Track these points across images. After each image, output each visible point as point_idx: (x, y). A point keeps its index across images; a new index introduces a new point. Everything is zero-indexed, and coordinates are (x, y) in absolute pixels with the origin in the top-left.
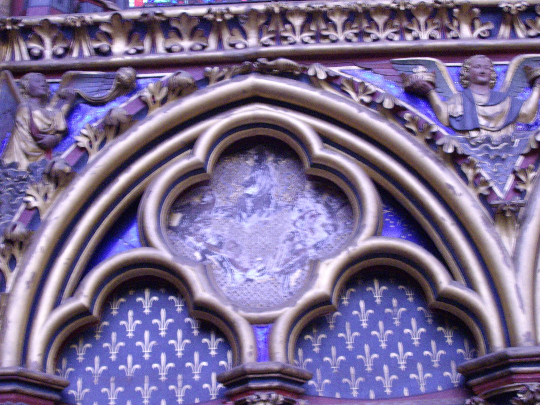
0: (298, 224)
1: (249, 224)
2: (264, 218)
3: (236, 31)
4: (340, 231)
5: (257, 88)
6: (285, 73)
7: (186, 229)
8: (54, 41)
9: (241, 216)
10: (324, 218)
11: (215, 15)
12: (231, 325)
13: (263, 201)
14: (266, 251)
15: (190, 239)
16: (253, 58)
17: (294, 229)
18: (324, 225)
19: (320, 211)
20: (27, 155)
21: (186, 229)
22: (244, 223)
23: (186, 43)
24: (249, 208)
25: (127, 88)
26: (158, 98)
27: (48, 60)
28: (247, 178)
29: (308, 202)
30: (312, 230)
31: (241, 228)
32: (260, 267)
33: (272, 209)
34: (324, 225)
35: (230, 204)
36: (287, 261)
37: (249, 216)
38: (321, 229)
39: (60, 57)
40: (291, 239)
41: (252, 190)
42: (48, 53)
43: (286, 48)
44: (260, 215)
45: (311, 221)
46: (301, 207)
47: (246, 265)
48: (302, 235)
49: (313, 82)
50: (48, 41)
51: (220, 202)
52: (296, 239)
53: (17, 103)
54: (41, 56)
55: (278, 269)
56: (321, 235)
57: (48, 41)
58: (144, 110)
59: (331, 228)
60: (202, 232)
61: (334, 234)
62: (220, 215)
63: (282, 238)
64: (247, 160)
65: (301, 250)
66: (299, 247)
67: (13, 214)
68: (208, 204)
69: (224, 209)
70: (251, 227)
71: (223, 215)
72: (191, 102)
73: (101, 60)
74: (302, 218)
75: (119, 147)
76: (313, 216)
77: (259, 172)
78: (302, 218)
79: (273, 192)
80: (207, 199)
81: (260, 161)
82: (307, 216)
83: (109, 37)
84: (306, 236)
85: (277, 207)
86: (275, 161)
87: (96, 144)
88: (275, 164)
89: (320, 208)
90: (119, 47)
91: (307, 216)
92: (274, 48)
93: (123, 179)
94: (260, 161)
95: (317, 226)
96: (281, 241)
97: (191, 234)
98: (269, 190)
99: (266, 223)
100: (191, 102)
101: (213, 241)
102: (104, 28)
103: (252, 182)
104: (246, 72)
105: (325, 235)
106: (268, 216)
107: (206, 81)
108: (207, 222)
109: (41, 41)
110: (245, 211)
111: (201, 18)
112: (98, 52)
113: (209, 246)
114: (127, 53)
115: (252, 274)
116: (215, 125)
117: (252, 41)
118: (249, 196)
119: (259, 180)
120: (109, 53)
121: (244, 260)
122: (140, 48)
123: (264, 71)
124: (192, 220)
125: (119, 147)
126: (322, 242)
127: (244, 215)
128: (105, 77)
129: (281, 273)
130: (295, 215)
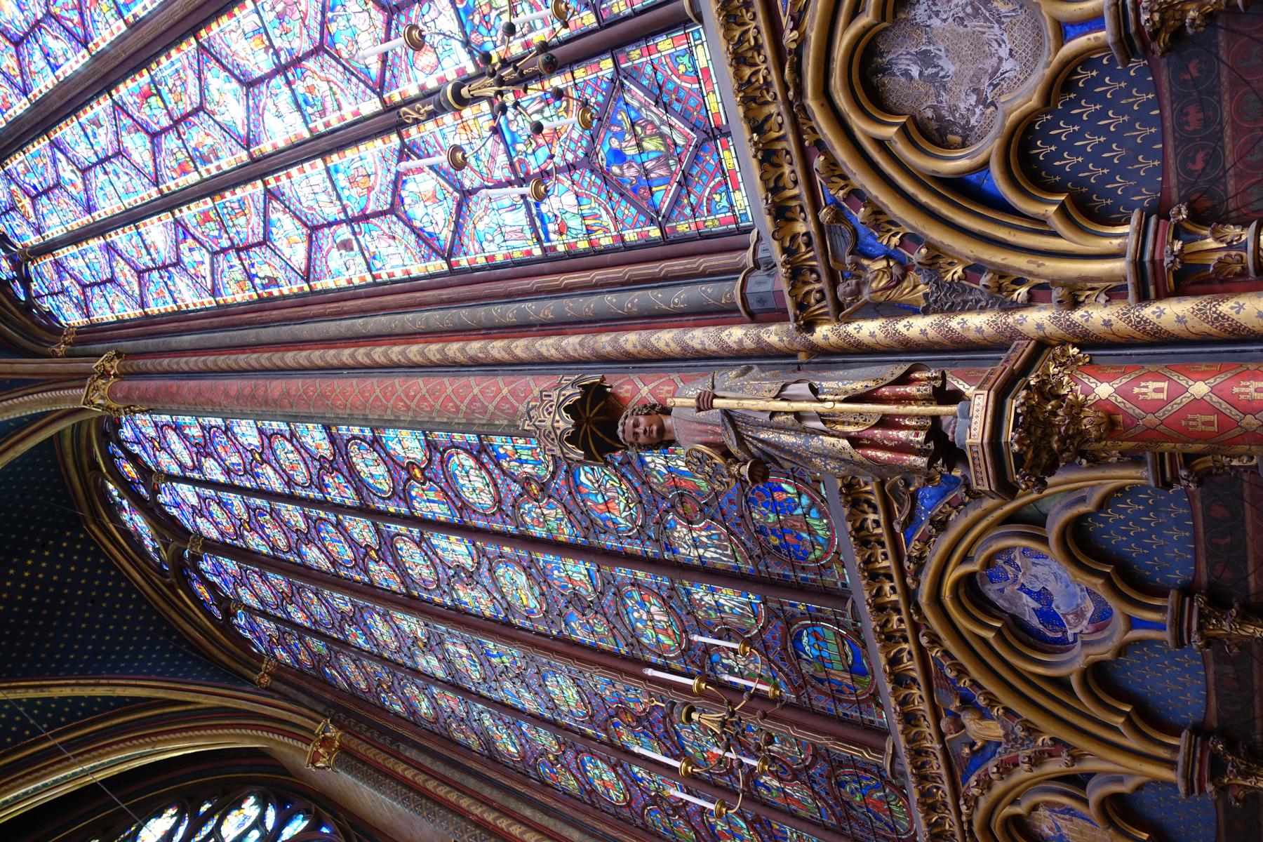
1: (950, 67)
2: (943, 54)
3: (766, 127)
5: (816, 97)
6: (798, 70)
7: (963, 127)
8: (806, 283)
9: (943, 77)
11: (757, 150)
12: (1065, 64)
13: (925, 58)
14: (978, 43)
15: (973, 122)
16: (789, 104)
17: (950, 20)
20: (915, 287)
21: (963, 127)
23: (787, 169)
24: (934, 70)
25: (839, 215)
26: (842, 183)
27: (824, 284)
31: (955, 74)
32: (995, 45)
33: (931, 48)
35: (932, 91)
36: (986, 20)
39: (819, 275)
40: (962, 19)
41: (915, 71)
42: (817, 286)
43: (773, 77)
44: (940, 58)
47: (994, 61)
49: (802, 41)
50: (807, 288)
51: (932, 101)
53: (866, 303)
54: (820, 291)
55: (996, 26)
57: (807, 288)
58: (857, 195)
62: (945, 97)
63: (961, 29)
64: (884, 85)
65: (973, 7)
66: (969, 10)
67: (972, 289)
72: (841, 153)
73: (816, 241)
74: (937, 14)
75: (895, 208)
78: (937, 14)
79: (913, 51)
80: (929, 113)
82: (934, 9)
83: (794, 237)
87: (895, 229)
90: (801, 228)
91: (934, 9)
92: (776, 88)
93: (924, 198)
97: (968, 122)
99: (947, 50)
100: (841, 153)
101: (973, 99)
102: (787, 244)
103: (906, 74)
104: (803, 108)
107: (820, 145)
108: (953, 109)
109: (809, 293)
110: (937, 74)
111: (761, 162)
112: (809, 244)
113: (978, 102)
114: (805, 219)
115: (1004, 52)
116: (859, 124)
117: (773, 109)
118: (921, 73)
119: (903, 67)
120: (807, 234)
121: (990, 63)
122: (798, 209)
123: (800, 92)
124: (954, 123)
125: (895, 208)
127: (942, 74)
128: (830, 233)
129: (1000, 22)
130: (936, 22)
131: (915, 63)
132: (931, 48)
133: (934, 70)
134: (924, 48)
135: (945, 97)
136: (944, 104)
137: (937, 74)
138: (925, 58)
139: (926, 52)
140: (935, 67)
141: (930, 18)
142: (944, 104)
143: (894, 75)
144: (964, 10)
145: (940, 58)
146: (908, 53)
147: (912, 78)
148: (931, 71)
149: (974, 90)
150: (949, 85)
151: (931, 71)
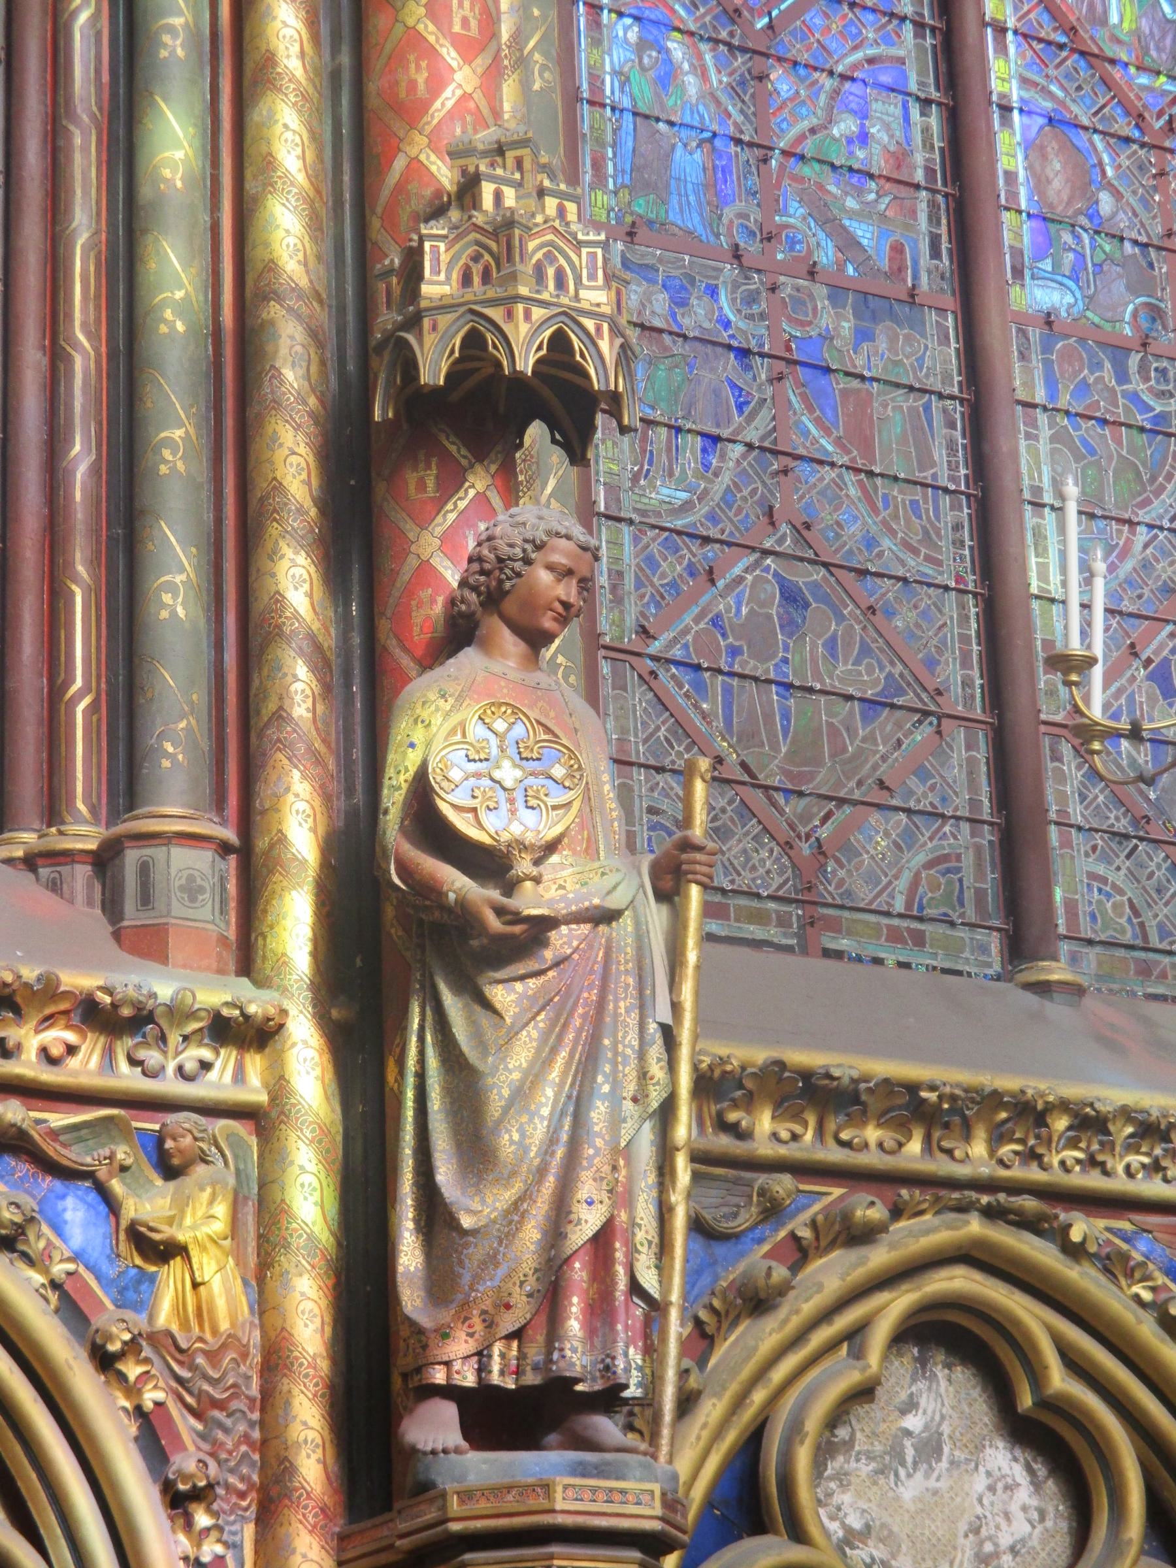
0: (985, 1502)
1: (911, 1489)
2: (932, 1483)
4: (1049, 1524)
9: (897, 1475)
10: (1024, 1494)
17: (979, 1510)
18: (1024, 1509)
19: (1019, 1479)
22: (902, 1489)
24: (909, 1460)
28: (903, 1396)
29: (1003, 1460)
30: (1007, 1516)
31: (897, 1498)
33: (944, 1464)
34: (1024, 1509)
37: (909, 1476)
38: (1021, 1515)
40: (977, 1531)
41: (913, 1422)
44: (927, 1476)
45: (1005, 1497)
46: (989, 1467)
48: (992, 1524)
52: (984, 1532)
56: (1021, 1527)
59: (1035, 1516)
60: (837, 1499)
61: (1039, 1528)
62: (865, 1468)
63: (963, 1527)
66: (988, 1547)
68: (844, 1443)
69: (870, 1457)
70: (915, 1500)
71: (870, 1468)
76: (1007, 1488)
77: (922, 1385)
78: (992, 1489)
79: (946, 1429)
81: (922, 1361)
82: (1000, 1486)
84: (998, 1527)
85: (953, 1463)
86: (948, 1366)
88: (946, 1371)
89: (1018, 1472)
91: (1000, 1486)
94: (922, 1361)
95: (1014, 1508)
96: (961, 1534)
98: (940, 1425)
99: (935, 1492)
101: (856, 1523)
103: (910, 1406)
105: (1027, 1528)
106: (940, 1477)
118: (908, 1433)
119: (923, 1402)
126: (1023, 1541)
127: (902, 1472)
130: (980, 1483)
131: (926, 1427)
132: (944, 1464)
133: (909, 1460)
134: (946, 1450)
135: (865, 1468)
136: (853, 1465)
137: (903, 1463)
138: (930, 1448)
139: (938, 1451)
140: (915, 1463)
141: (989, 1474)
142: (853, 1465)
143: (914, 1380)
144: (990, 1538)
145: (927, 1476)
146: (943, 1417)
147: (904, 1412)
148: (910, 1453)
149: (868, 1527)
150: (882, 1481)
151: (910, 1453)
